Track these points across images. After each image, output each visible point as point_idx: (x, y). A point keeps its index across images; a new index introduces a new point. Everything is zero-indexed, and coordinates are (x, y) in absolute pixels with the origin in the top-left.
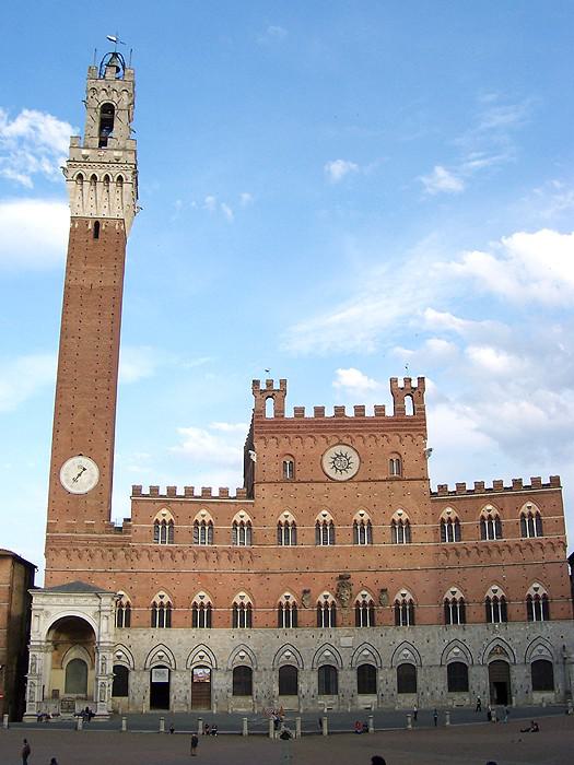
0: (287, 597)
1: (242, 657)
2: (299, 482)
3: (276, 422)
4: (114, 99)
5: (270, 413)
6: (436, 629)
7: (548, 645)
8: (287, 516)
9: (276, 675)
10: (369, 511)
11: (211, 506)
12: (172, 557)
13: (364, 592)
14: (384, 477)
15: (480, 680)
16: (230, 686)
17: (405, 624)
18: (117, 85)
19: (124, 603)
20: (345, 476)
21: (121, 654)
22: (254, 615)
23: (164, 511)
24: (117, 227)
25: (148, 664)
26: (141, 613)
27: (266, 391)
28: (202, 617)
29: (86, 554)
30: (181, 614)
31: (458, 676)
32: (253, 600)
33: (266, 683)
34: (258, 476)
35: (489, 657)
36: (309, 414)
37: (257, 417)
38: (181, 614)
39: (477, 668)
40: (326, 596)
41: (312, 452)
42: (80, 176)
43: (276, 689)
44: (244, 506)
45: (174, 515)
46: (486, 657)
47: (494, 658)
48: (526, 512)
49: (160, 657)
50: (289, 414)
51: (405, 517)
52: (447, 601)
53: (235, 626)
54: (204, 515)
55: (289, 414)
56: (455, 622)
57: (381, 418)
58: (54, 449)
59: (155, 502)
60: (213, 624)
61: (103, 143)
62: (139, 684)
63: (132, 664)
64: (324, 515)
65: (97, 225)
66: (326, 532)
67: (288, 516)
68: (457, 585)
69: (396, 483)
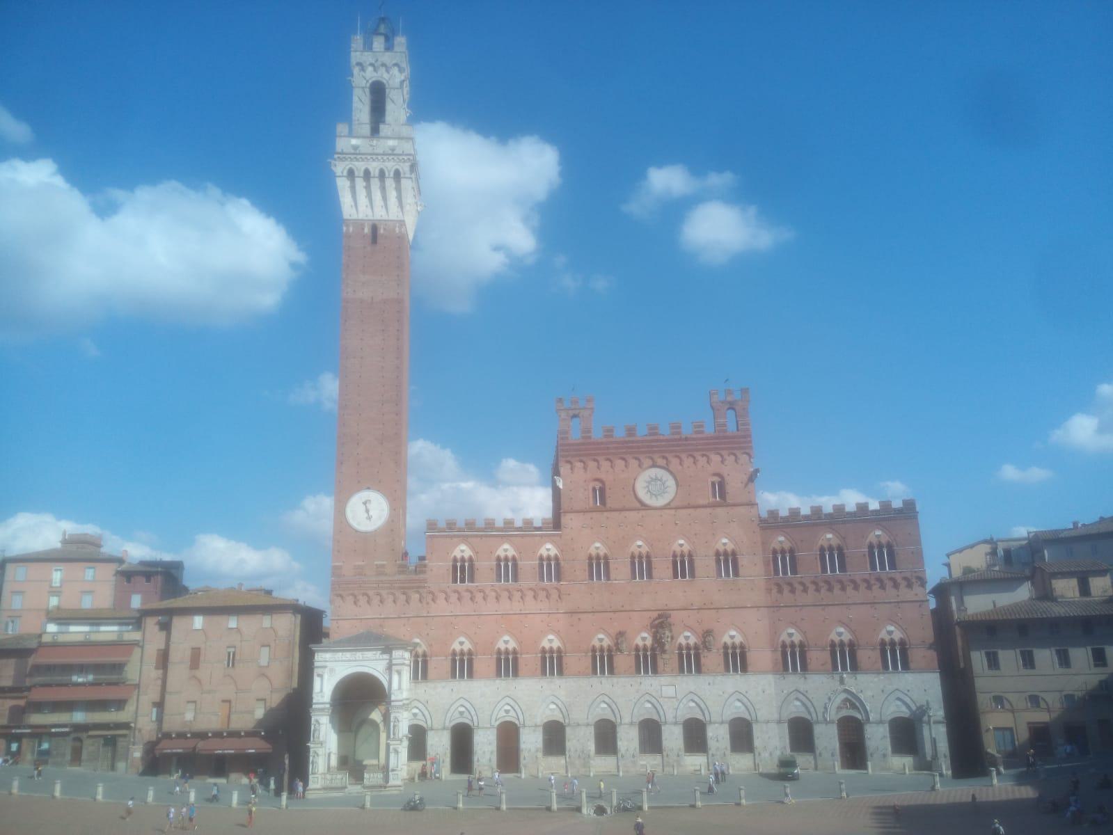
0: (601, 640)
3: (583, 444)
4: (383, 76)
6: (770, 677)
7: (907, 700)
8: (597, 548)
9: (592, 729)
13: (688, 634)
14: (705, 502)
15: (828, 738)
16: (540, 744)
17: (735, 670)
18: (387, 58)
19: (420, 651)
20: (660, 502)
21: (415, 711)
22: (565, 660)
23: (463, 547)
24: (397, 229)
25: (447, 722)
26: (439, 664)
28: (508, 665)
29: (376, 600)
30: (484, 663)
31: (801, 733)
32: (564, 645)
33: (581, 740)
34: (565, 505)
35: (837, 712)
37: (562, 439)
38: (484, 663)
39: (824, 726)
40: (644, 638)
43: (592, 747)
44: (549, 538)
45: (472, 548)
46: (833, 712)
47: (845, 713)
48: (875, 541)
49: (461, 713)
51: (730, 547)
52: (784, 646)
53: (544, 673)
54: (506, 550)
56: (795, 669)
57: (700, 436)
59: (452, 537)
60: (520, 673)
61: (375, 131)
62: (439, 745)
63: (429, 722)
64: (639, 545)
65: (374, 229)
66: (642, 566)
67: (598, 548)
68: (793, 624)
69: (720, 511)
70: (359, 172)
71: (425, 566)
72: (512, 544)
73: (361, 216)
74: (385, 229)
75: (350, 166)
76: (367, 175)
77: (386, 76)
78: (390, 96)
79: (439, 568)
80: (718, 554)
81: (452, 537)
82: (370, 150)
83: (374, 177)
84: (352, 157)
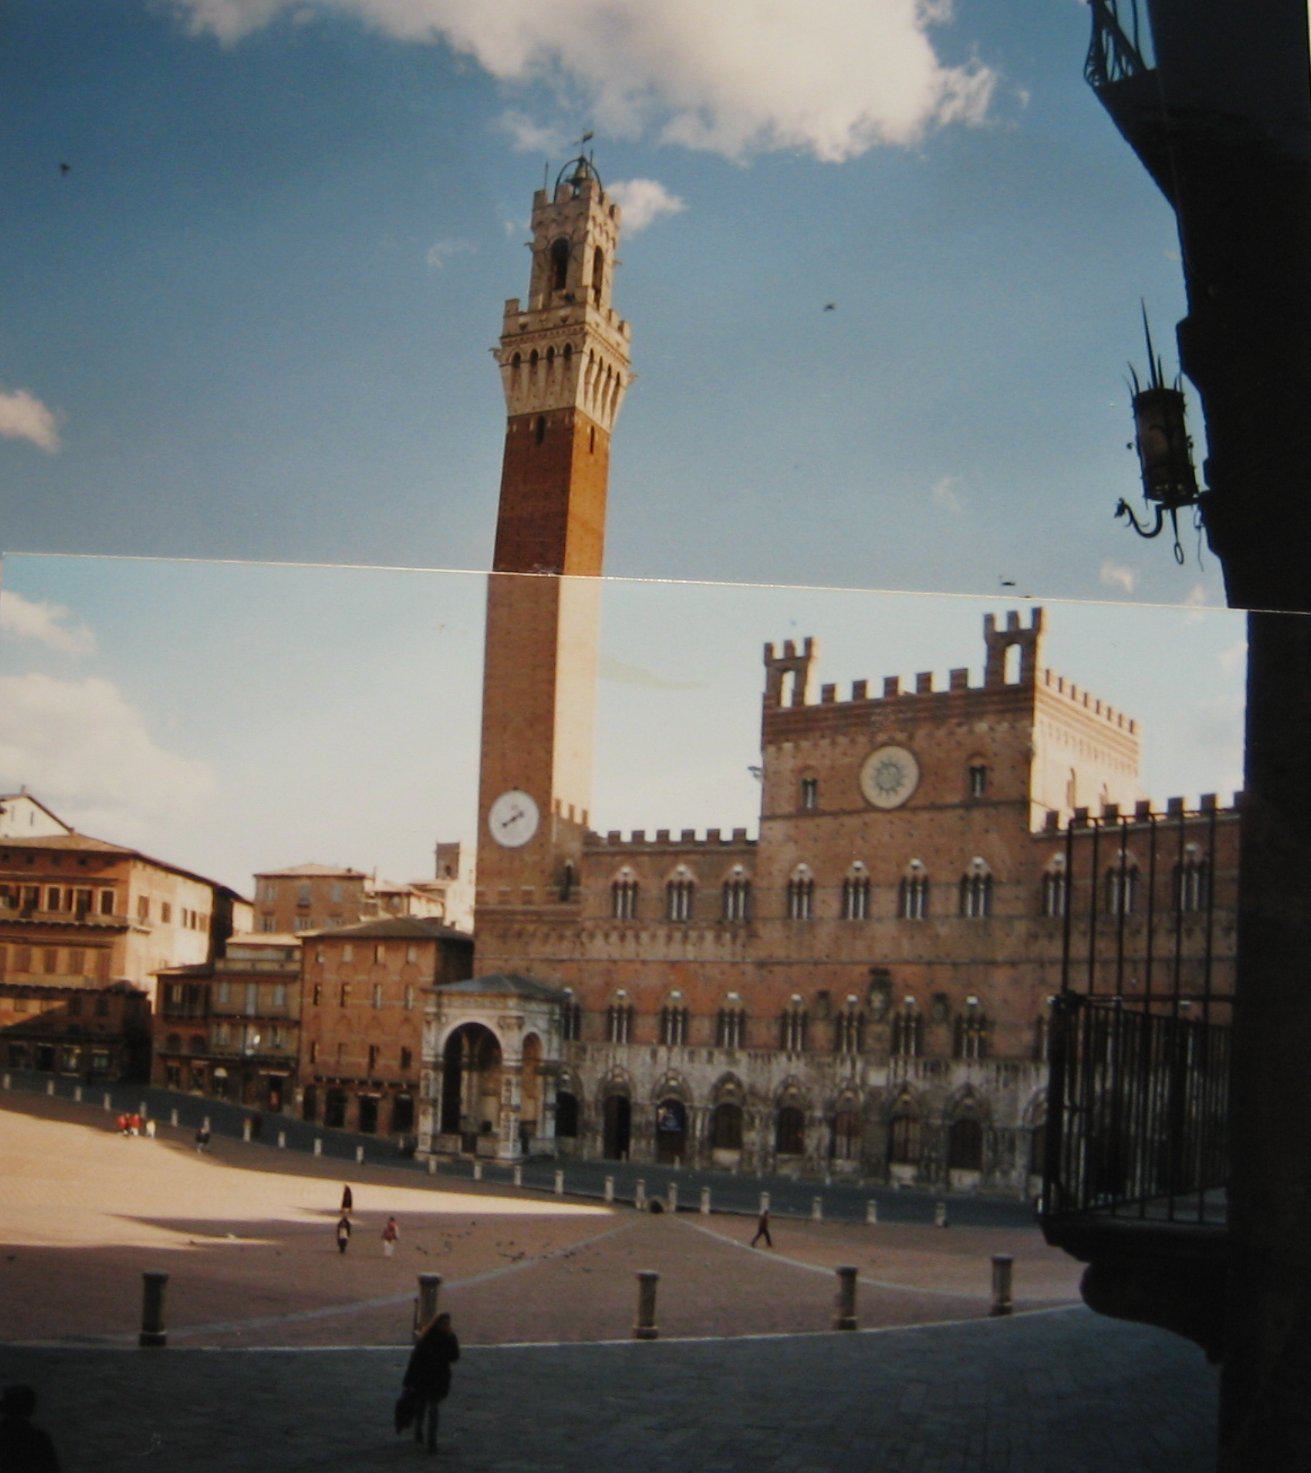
1: (730, 1092)
2: (824, 813)
5: (787, 701)
10: (925, 861)
11: (693, 857)
12: (637, 937)
20: (894, 800)
24: (567, 420)
27: (787, 663)
36: (844, 695)
41: (847, 760)
42: (517, 357)
50: (813, 697)
54: (683, 871)
55: (813, 697)
58: (483, 781)
67: (804, 871)
70: (526, 356)
71: (577, 893)
72: (686, 863)
73: (528, 410)
74: (553, 423)
75: (517, 350)
76: (534, 354)
77: (569, 230)
78: (573, 252)
79: (592, 892)
80: (965, 879)
81: (614, 854)
82: (538, 326)
83: (542, 359)
84: (518, 338)
